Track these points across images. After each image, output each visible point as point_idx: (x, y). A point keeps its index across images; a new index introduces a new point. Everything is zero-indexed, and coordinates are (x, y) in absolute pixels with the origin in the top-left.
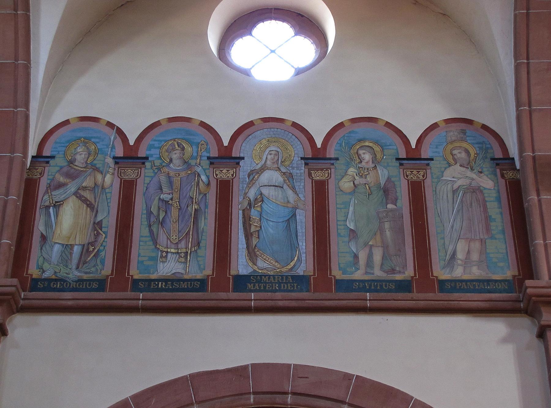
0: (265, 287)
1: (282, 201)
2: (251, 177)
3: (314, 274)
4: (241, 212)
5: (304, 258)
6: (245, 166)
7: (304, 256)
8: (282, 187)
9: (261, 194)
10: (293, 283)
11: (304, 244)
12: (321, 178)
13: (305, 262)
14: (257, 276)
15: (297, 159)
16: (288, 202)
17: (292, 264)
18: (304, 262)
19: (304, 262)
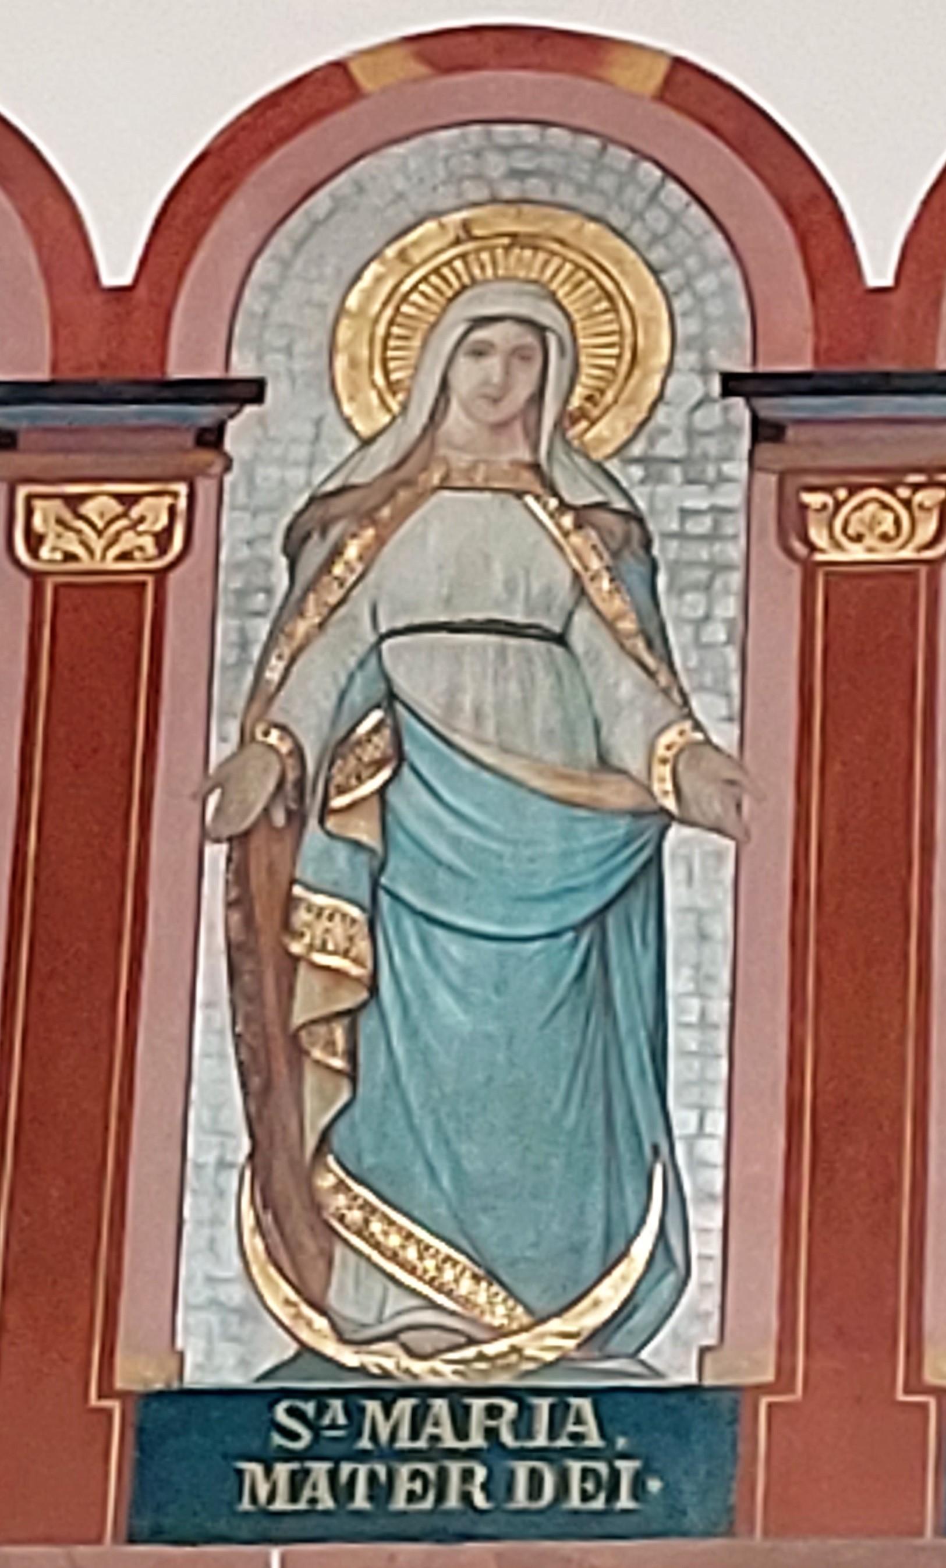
0: (381, 1491)
1: (554, 756)
2: (314, 554)
3: (784, 1379)
4: (216, 854)
5: (706, 1245)
6: (273, 461)
7: (705, 1220)
8: (561, 640)
9: (392, 696)
10: (609, 1454)
11: (717, 1122)
12: (886, 553)
13: (712, 1273)
14: (321, 1397)
15: (686, 386)
16: (604, 762)
17: (611, 1293)
18: (705, 1273)
19: (705, 1273)
